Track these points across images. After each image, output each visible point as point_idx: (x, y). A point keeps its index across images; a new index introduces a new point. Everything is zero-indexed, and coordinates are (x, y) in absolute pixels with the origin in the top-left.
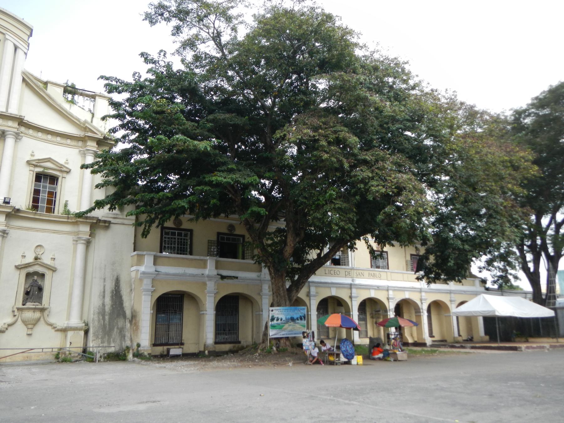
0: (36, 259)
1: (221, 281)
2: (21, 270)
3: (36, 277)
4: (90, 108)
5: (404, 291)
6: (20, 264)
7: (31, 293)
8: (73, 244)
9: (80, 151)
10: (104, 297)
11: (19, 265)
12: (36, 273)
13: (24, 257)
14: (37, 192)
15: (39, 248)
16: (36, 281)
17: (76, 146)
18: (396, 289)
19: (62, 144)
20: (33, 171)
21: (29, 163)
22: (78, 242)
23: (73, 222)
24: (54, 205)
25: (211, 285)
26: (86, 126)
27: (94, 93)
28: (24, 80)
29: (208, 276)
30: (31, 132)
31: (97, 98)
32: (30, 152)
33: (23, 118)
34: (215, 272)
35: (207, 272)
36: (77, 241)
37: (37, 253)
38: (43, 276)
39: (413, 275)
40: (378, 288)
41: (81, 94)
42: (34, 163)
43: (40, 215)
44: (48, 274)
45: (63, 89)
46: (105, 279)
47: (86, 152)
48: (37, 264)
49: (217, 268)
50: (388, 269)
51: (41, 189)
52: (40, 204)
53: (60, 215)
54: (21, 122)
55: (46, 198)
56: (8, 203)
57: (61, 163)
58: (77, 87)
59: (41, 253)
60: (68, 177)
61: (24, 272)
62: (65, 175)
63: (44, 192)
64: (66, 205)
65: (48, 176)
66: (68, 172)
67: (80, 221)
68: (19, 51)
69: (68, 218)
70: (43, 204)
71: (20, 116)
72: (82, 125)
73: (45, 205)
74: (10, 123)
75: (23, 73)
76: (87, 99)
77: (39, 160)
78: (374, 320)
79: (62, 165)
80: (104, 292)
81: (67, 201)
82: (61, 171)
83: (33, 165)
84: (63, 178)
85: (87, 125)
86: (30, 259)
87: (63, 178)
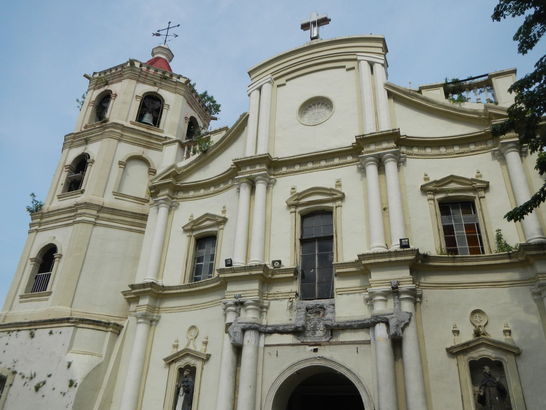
0: (477, 334)
2: (459, 357)
3: (487, 369)
4: (488, 98)
6: (453, 345)
7: (488, 401)
8: (535, 300)
9: (493, 154)
11: (452, 348)
12: (485, 361)
13: (456, 332)
14: (448, 230)
15: (477, 315)
16: (490, 375)
17: (486, 149)
19: (463, 153)
20: (433, 200)
21: (424, 190)
22: (542, 296)
23: (521, 262)
24: (482, 244)
26: (490, 113)
27: (487, 77)
28: (390, 95)
30: (415, 150)
31: (494, 80)
32: (424, 176)
33: (398, 131)
36: (539, 294)
37: (477, 325)
38: (498, 365)
41: (471, 88)
42: (431, 187)
43: (463, 259)
44: (508, 361)
45: (442, 89)
47: (502, 150)
48: (483, 344)
51: (453, 224)
52: (458, 247)
53: (494, 254)
55: (465, 235)
56: (408, 246)
57: (470, 177)
58: (460, 79)
59: (483, 324)
60: (487, 195)
61: (464, 361)
62: (482, 193)
63: (459, 227)
64: (499, 238)
65: (458, 203)
66: (486, 187)
67: (532, 255)
69: (509, 256)
70: (463, 246)
71: (393, 130)
72: (483, 117)
73: (467, 246)
74: (385, 145)
75: (387, 85)
76: (481, 92)
77: (436, 182)
79: (473, 180)
81: (499, 230)
82: (475, 190)
83: (431, 191)
84: (480, 198)
85: (490, 111)
86: (467, 336)
87: (480, 198)
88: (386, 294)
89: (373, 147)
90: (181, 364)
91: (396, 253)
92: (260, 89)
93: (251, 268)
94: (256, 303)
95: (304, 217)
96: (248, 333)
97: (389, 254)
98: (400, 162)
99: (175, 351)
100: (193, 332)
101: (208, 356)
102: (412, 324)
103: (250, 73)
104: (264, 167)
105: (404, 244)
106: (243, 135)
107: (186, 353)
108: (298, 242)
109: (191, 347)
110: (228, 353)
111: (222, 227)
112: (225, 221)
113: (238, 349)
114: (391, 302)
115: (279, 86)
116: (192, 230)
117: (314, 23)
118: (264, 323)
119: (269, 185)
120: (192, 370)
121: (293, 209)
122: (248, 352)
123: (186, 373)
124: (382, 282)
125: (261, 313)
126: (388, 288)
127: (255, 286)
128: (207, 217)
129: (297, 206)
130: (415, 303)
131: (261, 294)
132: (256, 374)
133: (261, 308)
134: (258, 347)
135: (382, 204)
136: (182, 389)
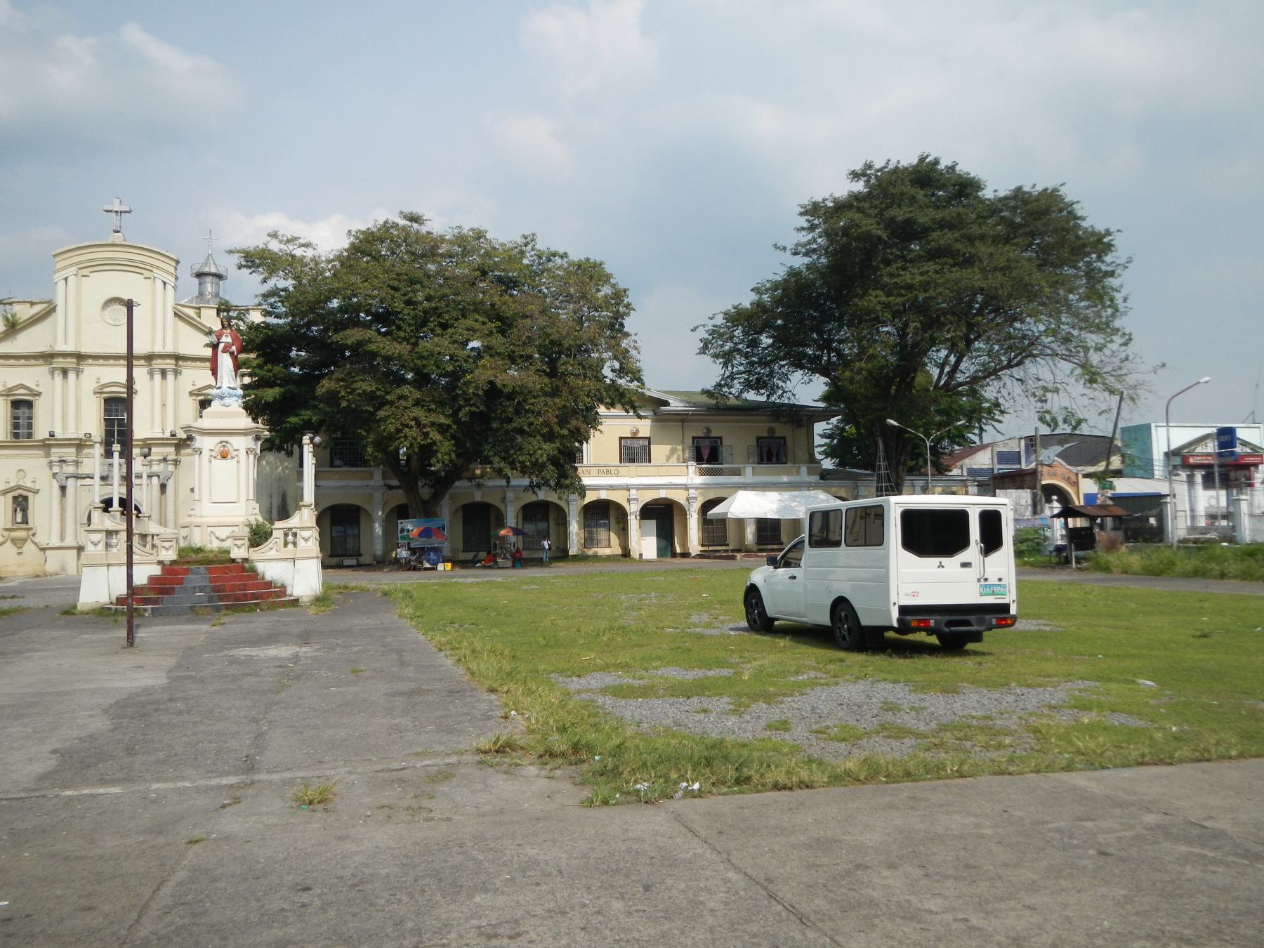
1: (388, 491)
5: (658, 489)
10: (271, 512)
18: (640, 488)
21: (191, 394)
25: (378, 496)
28: (175, 314)
29: (373, 487)
34: (382, 483)
35: (372, 483)
39: (693, 467)
40: (611, 488)
45: (216, 310)
46: (271, 496)
49: (384, 478)
50: (650, 462)
54: (177, 358)
56: (174, 435)
68: (167, 286)
74: (168, 361)
78: (621, 526)
80: (271, 508)
88: (160, 461)
89: (159, 361)
90: (16, 493)
91: (168, 439)
92: (66, 279)
93: (70, 439)
94: (75, 461)
95: (107, 401)
96: (69, 480)
97: (164, 439)
98: (176, 373)
99: (8, 486)
100: (21, 473)
101: (38, 491)
102: (172, 477)
103: (54, 256)
104: (74, 360)
105: (173, 435)
106: (50, 319)
107: (19, 487)
108: (103, 420)
109: (21, 483)
110: (56, 491)
111: (37, 398)
112: (39, 394)
113: (63, 489)
114: (162, 465)
115: (83, 276)
116: (7, 395)
117: (117, 212)
118: (80, 472)
119: (78, 372)
120: (26, 498)
121: (98, 395)
122: (70, 490)
123: (20, 500)
124: (158, 454)
125: (77, 466)
126: (161, 458)
127: (73, 450)
128: (22, 386)
129: (101, 393)
130: (176, 465)
131: (77, 455)
132: (76, 502)
133: (77, 463)
134: (76, 487)
135: (162, 401)
136: (18, 509)
